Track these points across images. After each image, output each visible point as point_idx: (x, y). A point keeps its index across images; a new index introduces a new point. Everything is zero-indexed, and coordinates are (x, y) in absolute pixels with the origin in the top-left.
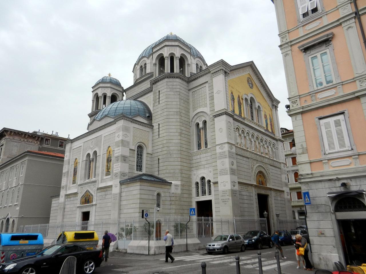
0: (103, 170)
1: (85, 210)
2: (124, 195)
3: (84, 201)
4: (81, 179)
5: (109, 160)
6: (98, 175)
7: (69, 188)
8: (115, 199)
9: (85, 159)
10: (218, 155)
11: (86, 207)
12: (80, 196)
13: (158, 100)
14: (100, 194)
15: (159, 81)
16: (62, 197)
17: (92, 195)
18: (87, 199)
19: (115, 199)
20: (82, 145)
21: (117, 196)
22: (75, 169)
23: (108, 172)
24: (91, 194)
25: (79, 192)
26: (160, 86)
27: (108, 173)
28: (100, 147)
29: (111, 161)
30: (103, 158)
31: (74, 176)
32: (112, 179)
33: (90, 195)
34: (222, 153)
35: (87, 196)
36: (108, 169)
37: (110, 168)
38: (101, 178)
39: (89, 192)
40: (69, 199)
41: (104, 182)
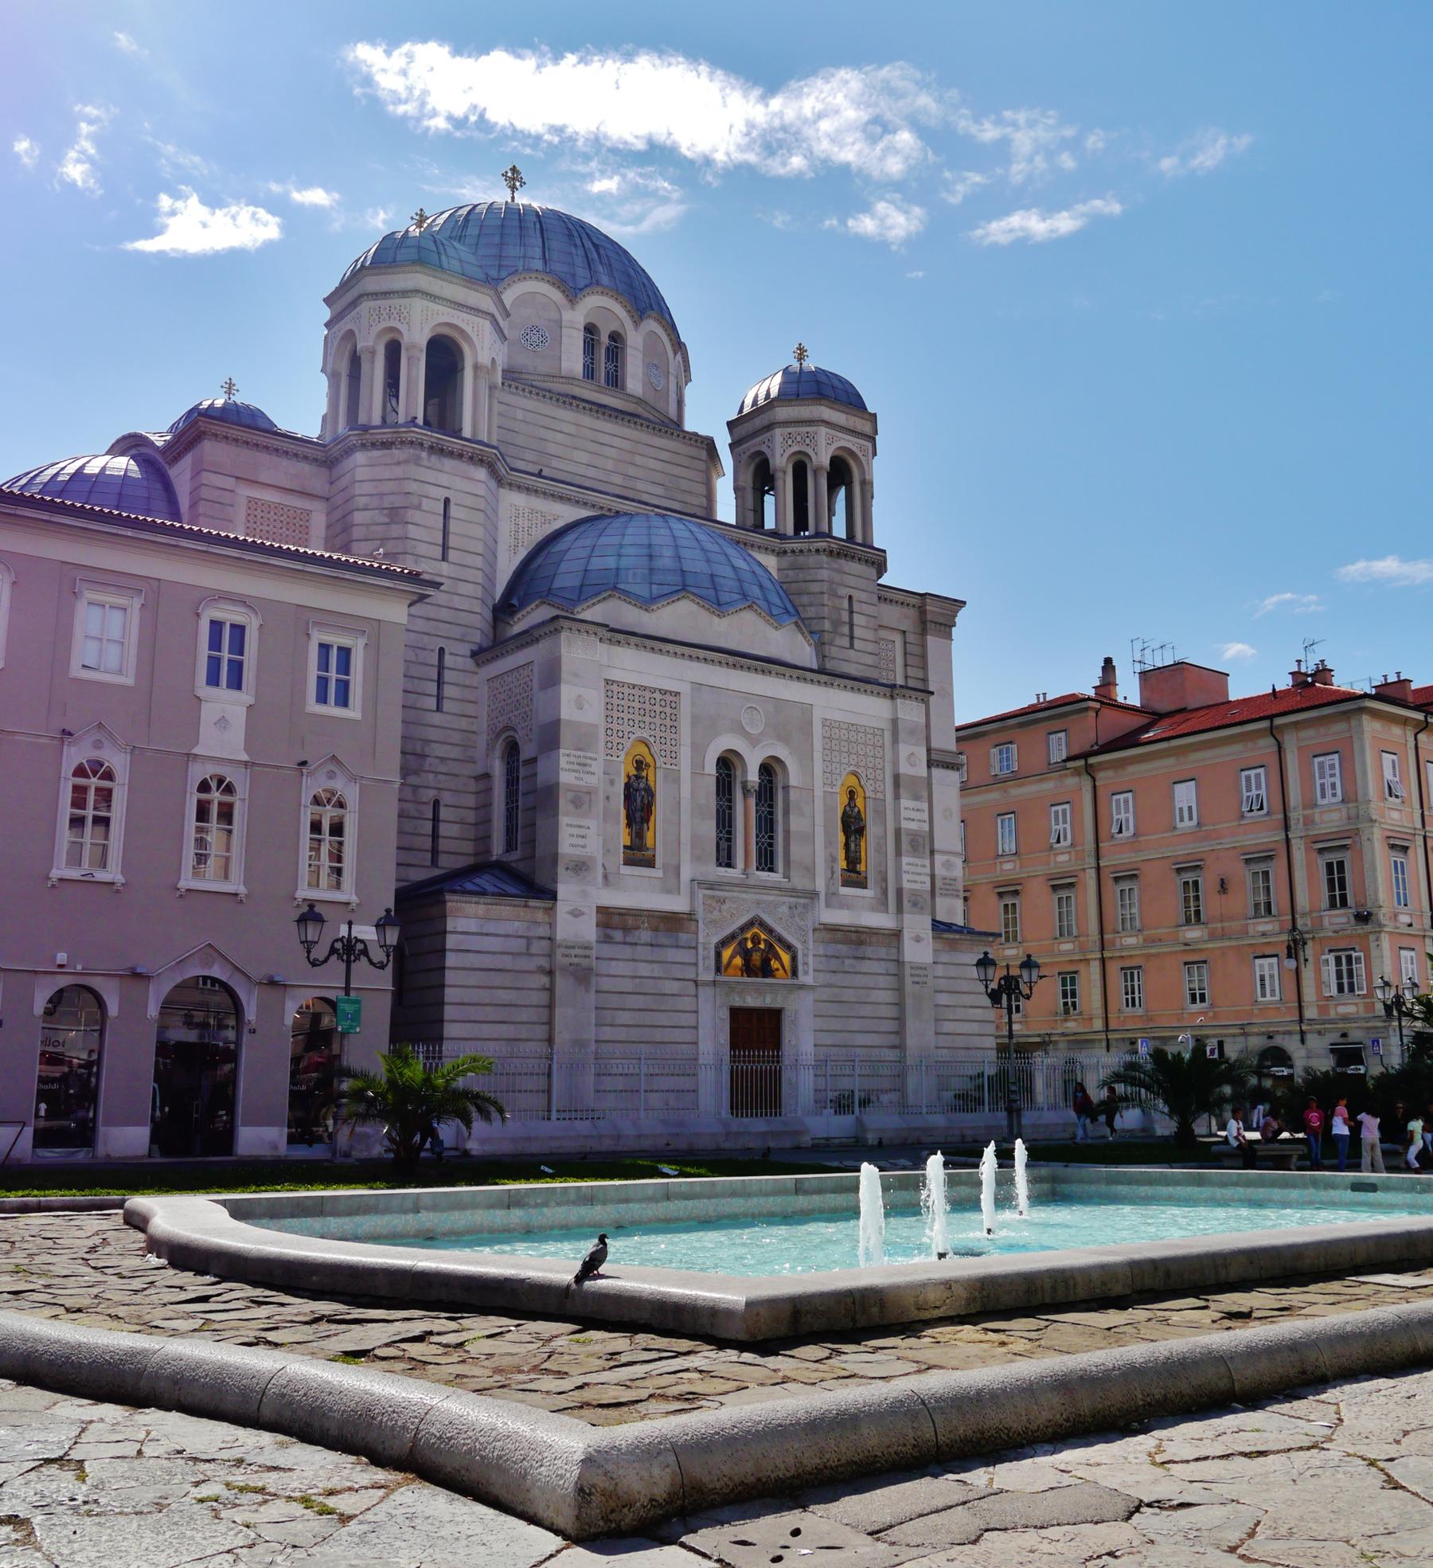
0: (834, 860)
1: (751, 1001)
2: (941, 975)
3: (738, 961)
4: (697, 858)
5: (853, 826)
6: (810, 870)
7: (605, 877)
8: (918, 983)
9: (711, 768)
10: (938, 884)
11: (759, 991)
12: (707, 937)
13: (846, 630)
14: (832, 949)
15: (853, 557)
16: (576, 914)
17: (789, 947)
18: (756, 958)
19: (918, 983)
20: (684, 689)
21: (925, 972)
22: (630, 791)
23: (848, 870)
24: (781, 940)
25: (700, 914)
26: (852, 581)
27: (853, 875)
28: (806, 757)
29: (861, 831)
30: (828, 810)
31: (629, 825)
32: (882, 904)
33: (771, 946)
34: (948, 881)
35: (756, 940)
36: (853, 860)
37: (858, 861)
38: (827, 886)
39: (770, 931)
40: (618, 935)
41: (841, 906)
